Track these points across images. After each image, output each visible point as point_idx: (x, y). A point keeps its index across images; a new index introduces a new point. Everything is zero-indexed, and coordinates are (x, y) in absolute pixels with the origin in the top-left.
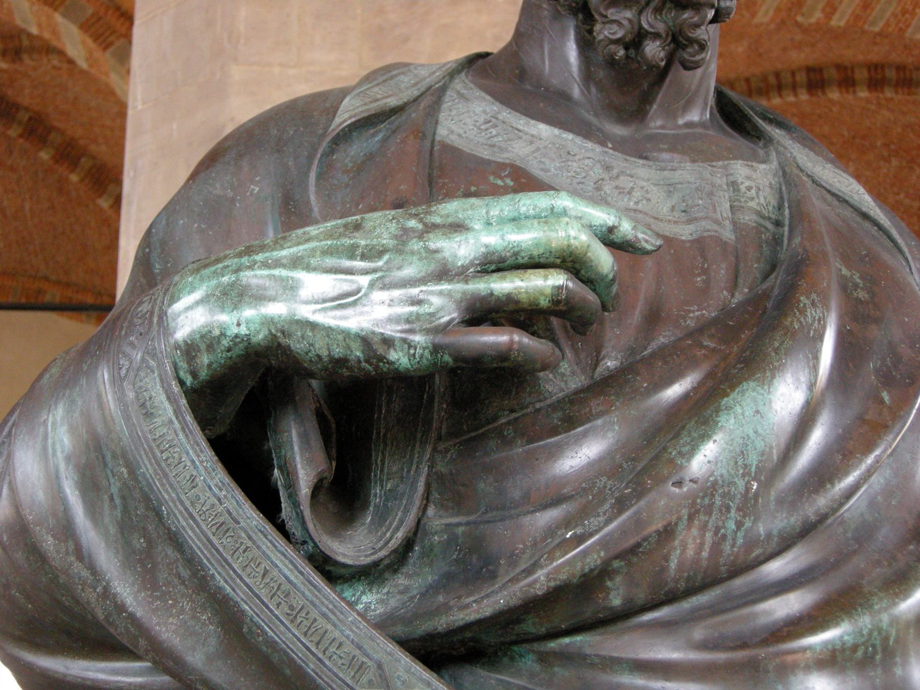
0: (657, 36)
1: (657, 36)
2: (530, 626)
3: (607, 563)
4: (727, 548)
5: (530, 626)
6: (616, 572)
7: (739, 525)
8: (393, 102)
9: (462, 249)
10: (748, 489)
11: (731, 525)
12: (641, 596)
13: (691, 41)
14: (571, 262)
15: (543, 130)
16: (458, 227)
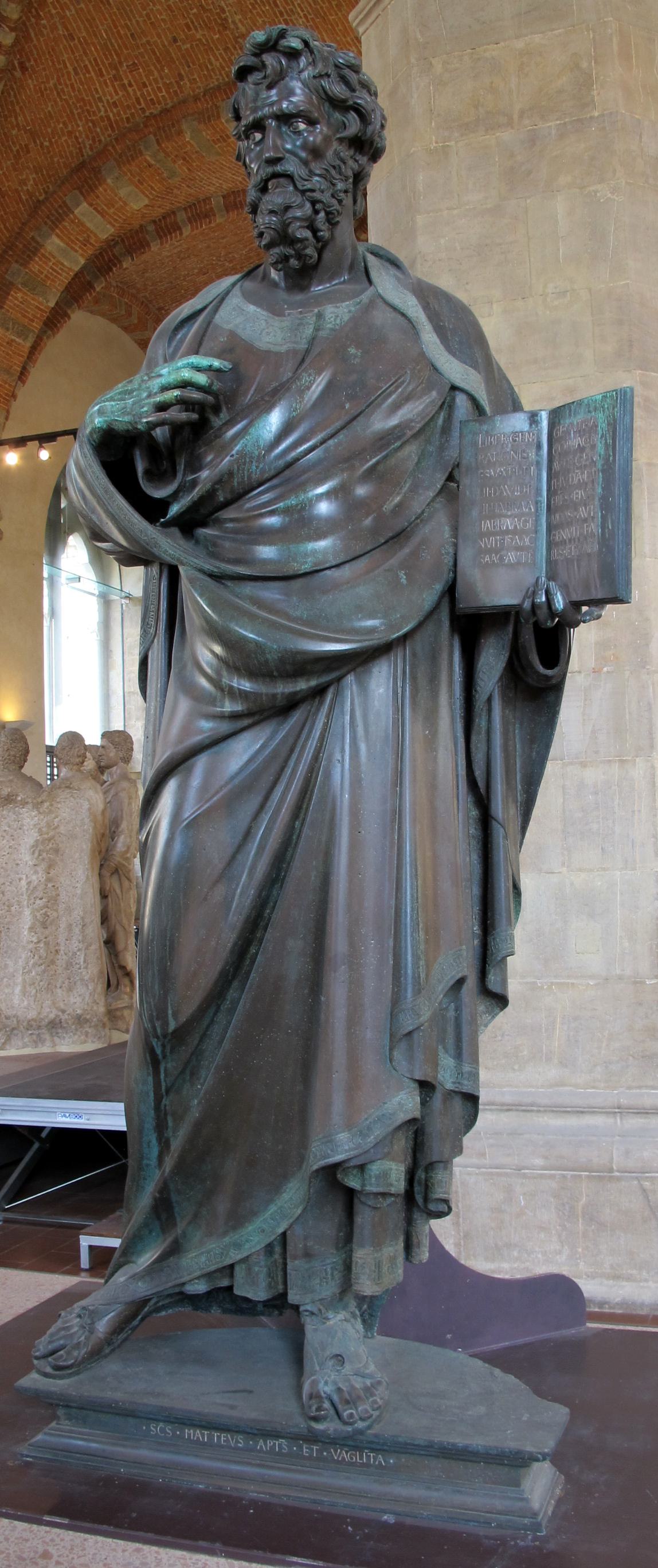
0: (292, 256)
1: (292, 256)
2: (203, 511)
3: (213, 486)
4: (254, 476)
5: (203, 511)
6: (217, 490)
7: (257, 467)
8: (199, 307)
9: (156, 384)
10: (260, 454)
11: (254, 468)
12: (229, 496)
13: (306, 255)
14: (185, 385)
15: (252, 308)
16: (160, 376)
